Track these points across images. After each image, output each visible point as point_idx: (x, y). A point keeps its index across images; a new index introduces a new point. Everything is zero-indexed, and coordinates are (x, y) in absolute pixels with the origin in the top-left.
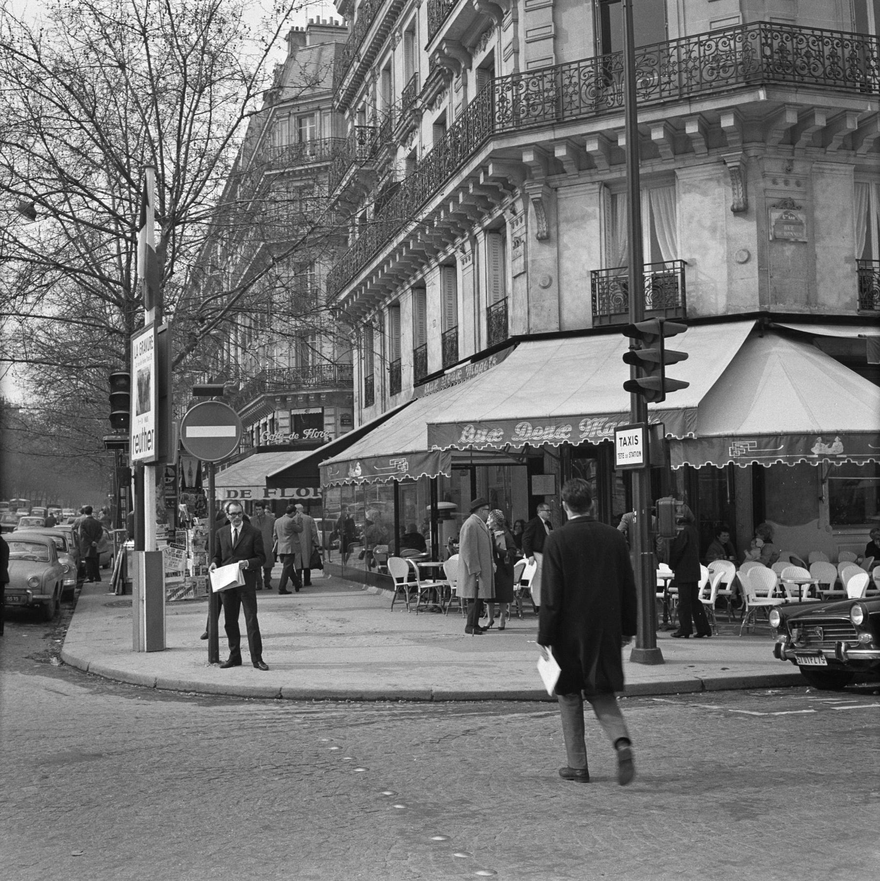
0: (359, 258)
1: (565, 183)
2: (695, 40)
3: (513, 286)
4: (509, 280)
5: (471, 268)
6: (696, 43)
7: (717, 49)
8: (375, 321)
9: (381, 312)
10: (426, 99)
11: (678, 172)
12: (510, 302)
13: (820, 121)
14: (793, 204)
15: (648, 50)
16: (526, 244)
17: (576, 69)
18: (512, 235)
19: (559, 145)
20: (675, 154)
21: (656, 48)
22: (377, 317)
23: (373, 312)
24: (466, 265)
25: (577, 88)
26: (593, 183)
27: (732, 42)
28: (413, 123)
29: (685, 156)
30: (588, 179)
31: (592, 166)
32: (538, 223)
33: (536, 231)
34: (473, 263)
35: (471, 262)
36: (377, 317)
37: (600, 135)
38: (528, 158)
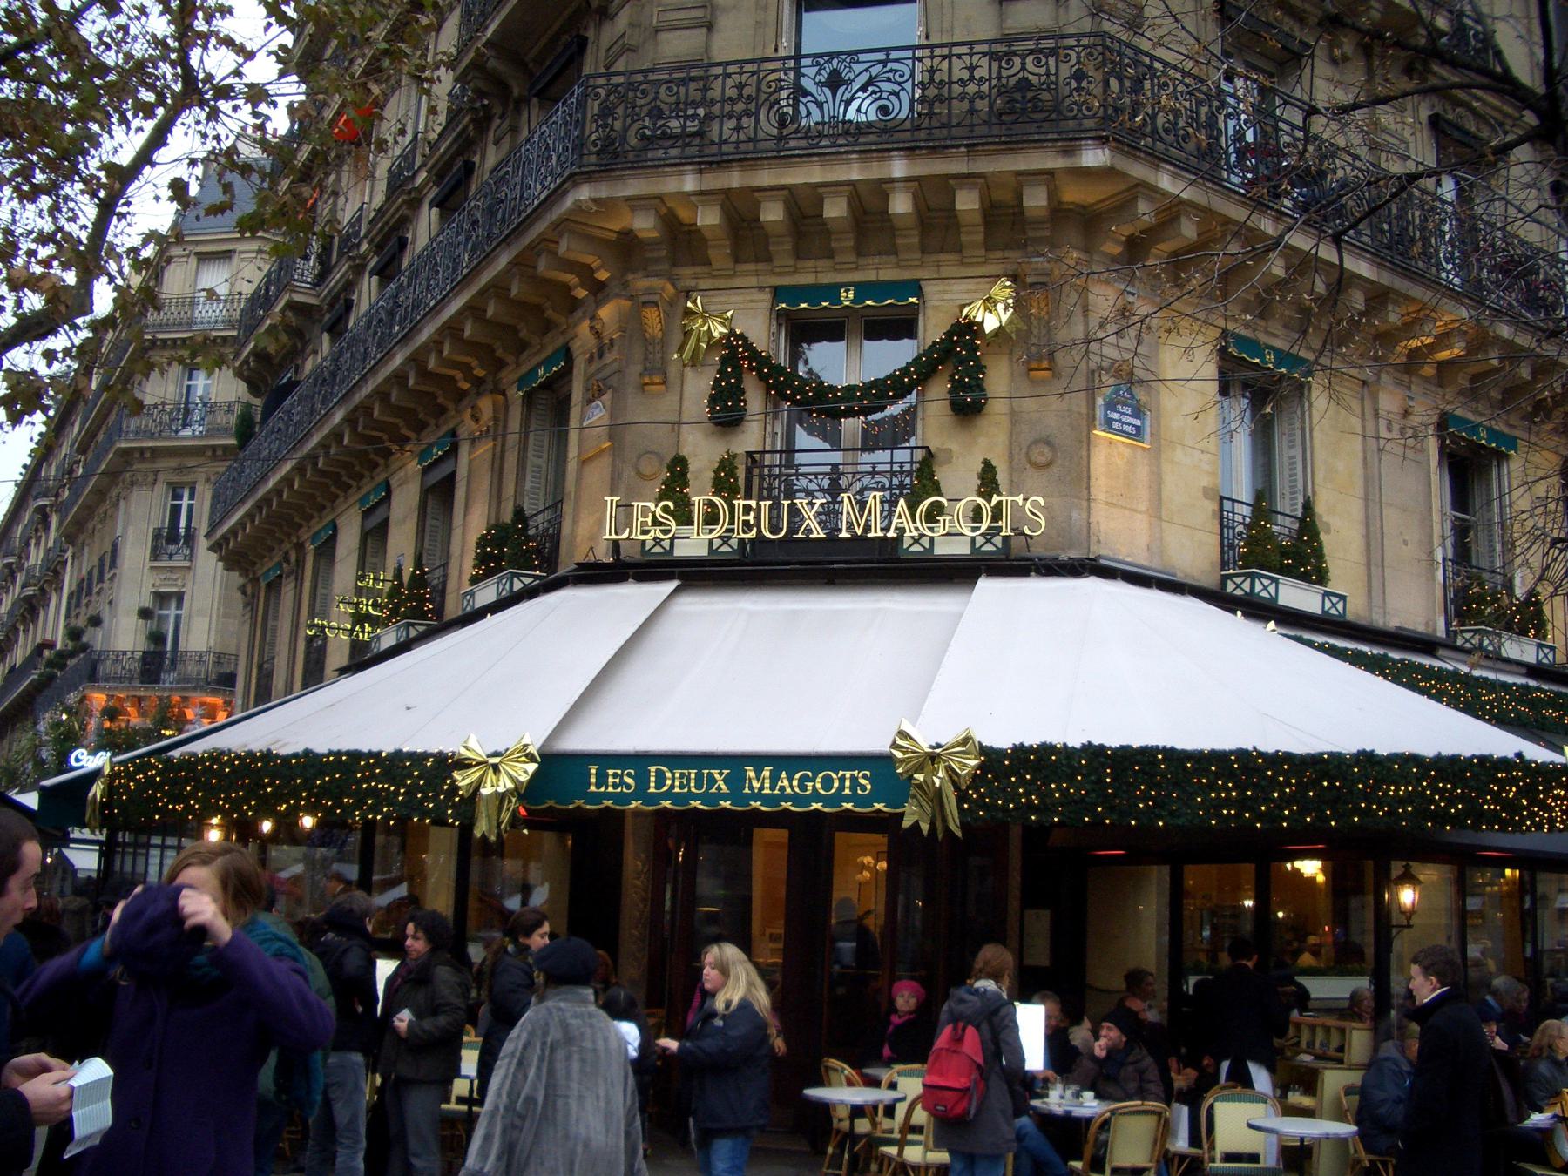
0: (275, 446)
1: (703, 284)
2: (984, 48)
3: (579, 479)
4: (572, 466)
6: (984, 54)
7: (1023, 68)
8: (288, 561)
9: (300, 547)
10: (433, 166)
11: (928, 288)
13: (1189, 230)
15: (894, 55)
17: (753, 73)
18: (587, 379)
19: (704, 204)
20: (923, 252)
21: (909, 54)
22: (293, 557)
23: (286, 546)
25: (752, 106)
26: (761, 288)
27: (1052, 61)
28: (404, 211)
29: (943, 257)
30: (753, 281)
31: (763, 255)
36: (293, 557)
37: (791, 196)
38: (644, 225)
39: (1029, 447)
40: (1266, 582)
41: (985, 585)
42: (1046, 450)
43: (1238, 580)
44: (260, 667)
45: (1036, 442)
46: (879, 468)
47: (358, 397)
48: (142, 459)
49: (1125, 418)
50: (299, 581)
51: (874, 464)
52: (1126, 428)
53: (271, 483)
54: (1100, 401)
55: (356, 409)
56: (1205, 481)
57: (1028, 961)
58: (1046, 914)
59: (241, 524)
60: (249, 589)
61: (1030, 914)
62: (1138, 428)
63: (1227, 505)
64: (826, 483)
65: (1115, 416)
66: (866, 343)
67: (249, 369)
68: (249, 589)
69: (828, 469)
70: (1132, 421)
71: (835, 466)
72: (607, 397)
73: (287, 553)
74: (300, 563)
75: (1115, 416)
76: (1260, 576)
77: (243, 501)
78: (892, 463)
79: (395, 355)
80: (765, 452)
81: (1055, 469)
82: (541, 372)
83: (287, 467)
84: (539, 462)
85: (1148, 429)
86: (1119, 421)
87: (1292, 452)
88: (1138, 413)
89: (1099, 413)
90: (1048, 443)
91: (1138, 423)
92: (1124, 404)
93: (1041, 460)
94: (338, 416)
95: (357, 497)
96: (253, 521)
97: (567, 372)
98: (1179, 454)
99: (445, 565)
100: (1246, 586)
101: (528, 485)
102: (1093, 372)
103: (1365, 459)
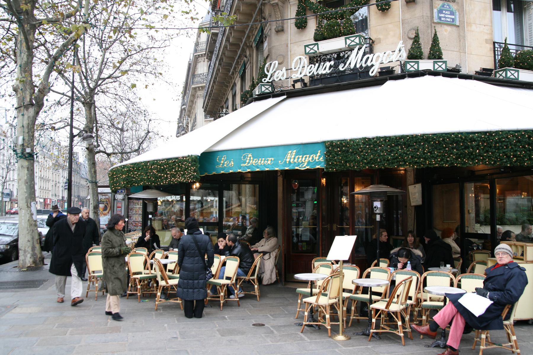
33: (275, 27)
39: (408, 33)
40: (513, 72)
43: (500, 73)
48: (199, 90)
52: (448, 19)
54: (435, 11)
56: (487, 37)
62: (453, 20)
65: (443, 15)
75: (443, 15)
76: (509, 70)
86: (445, 17)
88: (452, 13)
89: (435, 15)
91: (453, 17)
92: (446, 11)
98: (474, 27)
100: (504, 75)
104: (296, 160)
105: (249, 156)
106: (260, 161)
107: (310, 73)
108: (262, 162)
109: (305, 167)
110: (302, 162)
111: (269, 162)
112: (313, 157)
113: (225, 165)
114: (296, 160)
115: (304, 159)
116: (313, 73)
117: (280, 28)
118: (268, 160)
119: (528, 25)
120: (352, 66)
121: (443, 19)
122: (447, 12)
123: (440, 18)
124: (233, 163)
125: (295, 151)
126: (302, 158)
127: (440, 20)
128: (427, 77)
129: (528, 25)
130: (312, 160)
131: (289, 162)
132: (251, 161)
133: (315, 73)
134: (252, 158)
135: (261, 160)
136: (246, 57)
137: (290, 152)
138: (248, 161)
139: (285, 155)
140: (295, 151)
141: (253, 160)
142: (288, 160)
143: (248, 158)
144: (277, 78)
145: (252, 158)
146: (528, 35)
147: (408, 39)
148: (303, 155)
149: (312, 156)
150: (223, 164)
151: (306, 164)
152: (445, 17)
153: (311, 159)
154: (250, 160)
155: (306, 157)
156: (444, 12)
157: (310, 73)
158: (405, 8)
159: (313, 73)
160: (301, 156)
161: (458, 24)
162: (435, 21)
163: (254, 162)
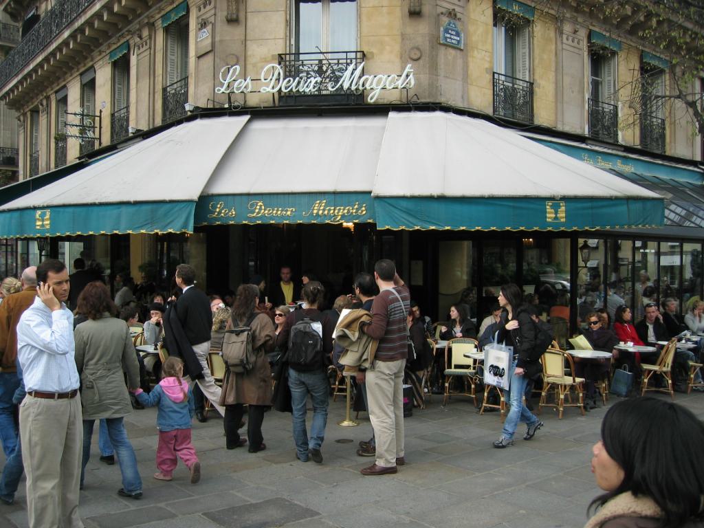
5: (148, 52)
8: (42, 105)
9: (48, 98)
12: (191, 81)
14: (455, 15)
16: (214, 25)
18: (198, 18)
22: (45, 102)
24: (142, 50)
32: (228, 6)
33: (225, 13)
34: (150, 48)
35: (148, 46)
36: (45, 102)
41: (392, 115)
42: (418, 53)
44: (31, 156)
45: (413, 48)
46: (341, 61)
47: (77, 24)
49: (452, 37)
50: (49, 114)
51: (338, 60)
52: (453, 41)
53: (31, 67)
54: (442, 29)
55: (76, 31)
56: (487, 65)
57: (413, 283)
58: (420, 263)
59: (16, 86)
60: (22, 118)
61: (413, 262)
63: (496, 76)
64: (316, 68)
66: (331, 4)
67: (11, 8)
68: (22, 118)
69: (317, 62)
70: (455, 38)
71: (320, 61)
72: (209, 27)
73: (41, 100)
74: (49, 105)
75: (449, 36)
77: (16, 75)
78: (347, 59)
79: (95, 4)
80: (286, 54)
81: (421, 61)
82: (173, 15)
83: (39, 59)
84: (173, 57)
85: (463, 42)
86: (450, 38)
87: (524, 51)
88: (458, 34)
90: (418, 49)
91: (458, 39)
93: (415, 57)
94: (66, 34)
95: (78, 73)
96: (22, 85)
97: (187, 16)
99: (128, 107)
101: (169, 69)
102: (438, 15)
103: (556, 54)
104: (326, 212)
105: (259, 204)
106: (275, 212)
107: (286, 89)
108: (279, 212)
109: (338, 221)
110: (335, 215)
111: (289, 213)
112: (349, 210)
113: (222, 215)
114: (326, 212)
115: (336, 211)
116: (292, 89)
117: (235, 16)
118: (287, 211)
119: (521, 53)
120: (346, 86)
121: (448, 40)
122: (453, 33)
123: (446, 38)
124: (234, 213)
125: (325, 201)
126: (334, 210)
127: (446, 41)
128: (438, 114)
129: (521, 53)
130: (347, 213)
131: (317, 214)
132: (263, 211)
133: (294, 90)
134: (263, 207)
135: (278, 210)
136: (141, 37)
137: (318, 202)
138: (257, 211)
139: (311, 206)
140: (325, 201)
141: (265, 210)
142: (315, 212)
143: (258, 207)
144: (238, 89)
145: (263, 207)
146: (521, 65)
147: (409, 60)
148: (335, 206)
149: (347, 208)
150: (220, 213)
151: (339, 217)
152: (450, 38)
153: (346, 211)
154: (260, 209)
155: (340, 209)
156: (450, 31)
157: (286, 89)
158: (407, 19)
159: (292, 89)
160: (333, 208)
161: (462, 48)
162: (441, 42)
163: (266, 212)
